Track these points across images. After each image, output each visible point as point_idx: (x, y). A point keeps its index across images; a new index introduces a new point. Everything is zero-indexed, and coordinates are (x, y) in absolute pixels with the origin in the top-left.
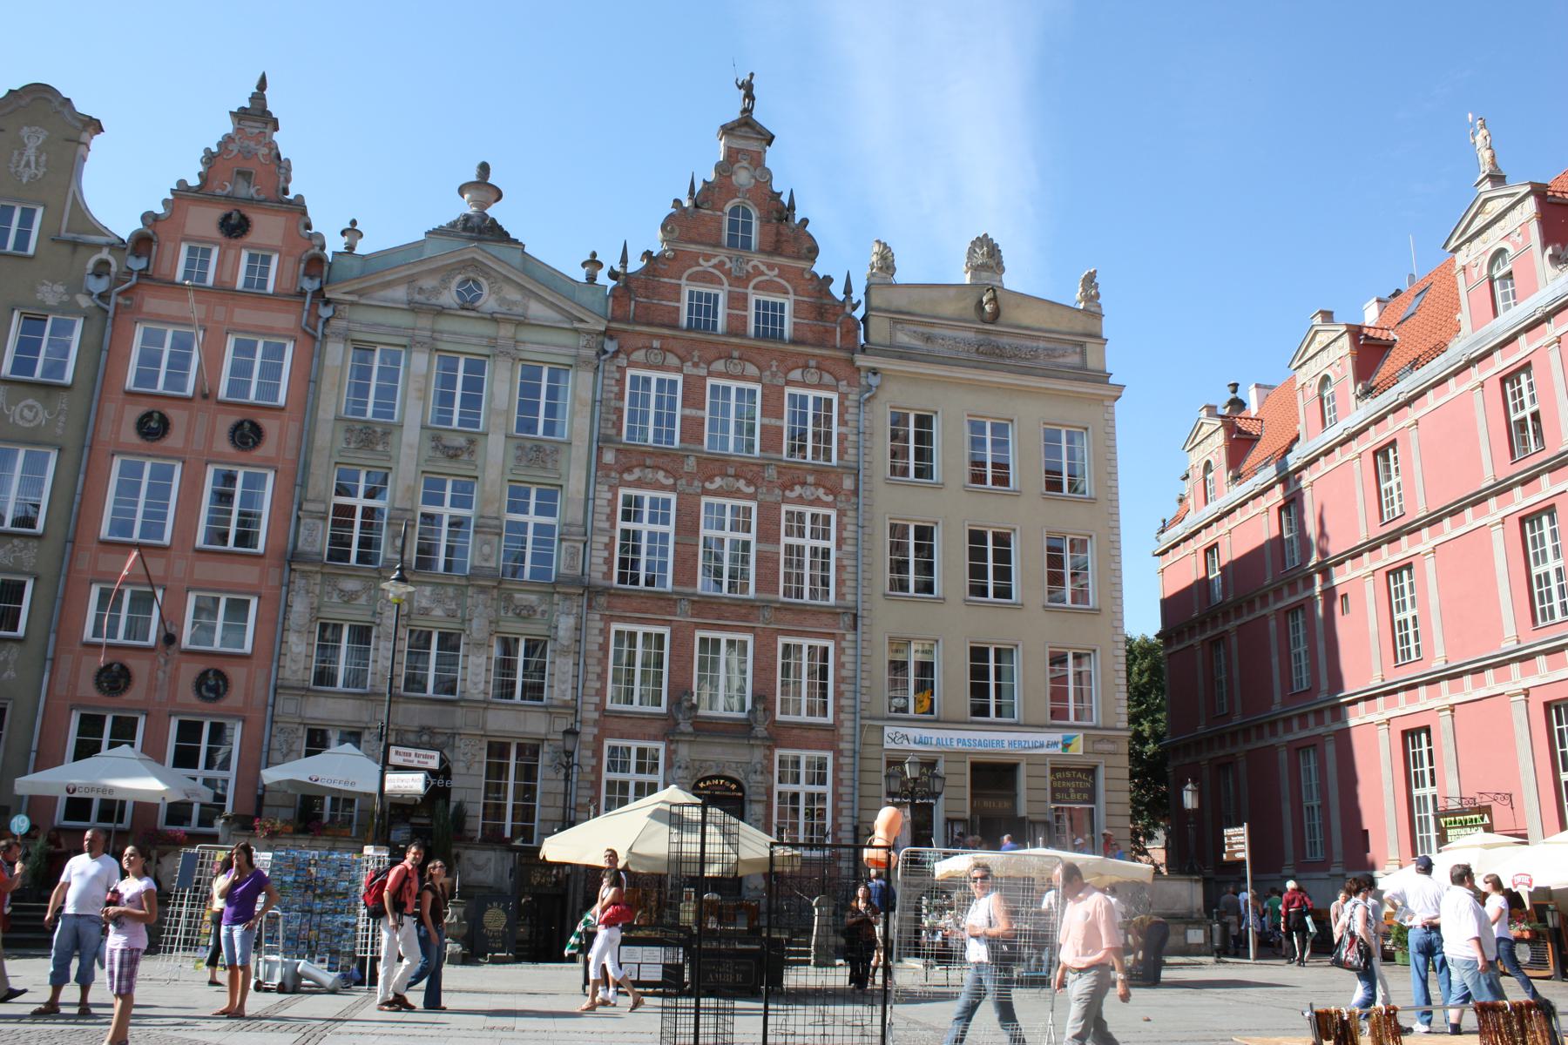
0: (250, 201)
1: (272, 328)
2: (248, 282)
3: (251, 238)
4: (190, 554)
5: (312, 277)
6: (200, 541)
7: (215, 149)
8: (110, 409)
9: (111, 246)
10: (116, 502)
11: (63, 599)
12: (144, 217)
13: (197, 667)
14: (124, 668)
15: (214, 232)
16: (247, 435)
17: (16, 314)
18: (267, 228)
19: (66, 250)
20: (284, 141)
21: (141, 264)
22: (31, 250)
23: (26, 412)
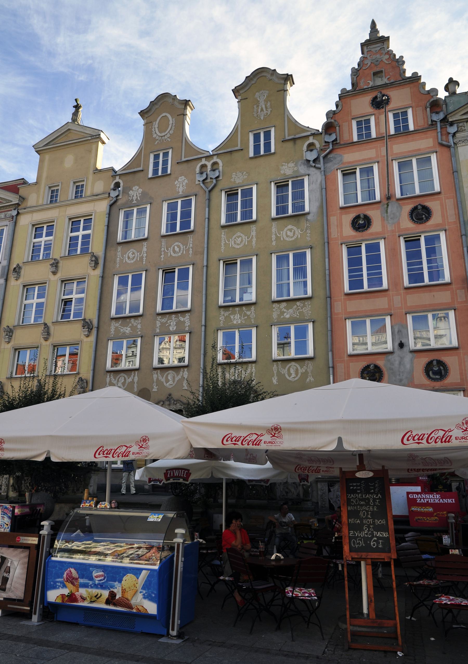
0: (385, 86)
1: (419, 150)
2: (397, 129)
3: (392, 105)
4: (402, 291)
5: (437, 113)
6: (406, 283)
7: (357, 67)
8: (333, 220)
9: (313, 135)
10: (350, 271)
11: (332, 331)
12: (328, 114)
13: (424, 360)
14: (376, 367)
15: (369, 109)
16: (421, 214)
17: (273, 184)
18: (399, 98)
19: (290, 144)
20: (395, 47)
21: (333, 137)
22: (273, 150)
23: (289, 233)
